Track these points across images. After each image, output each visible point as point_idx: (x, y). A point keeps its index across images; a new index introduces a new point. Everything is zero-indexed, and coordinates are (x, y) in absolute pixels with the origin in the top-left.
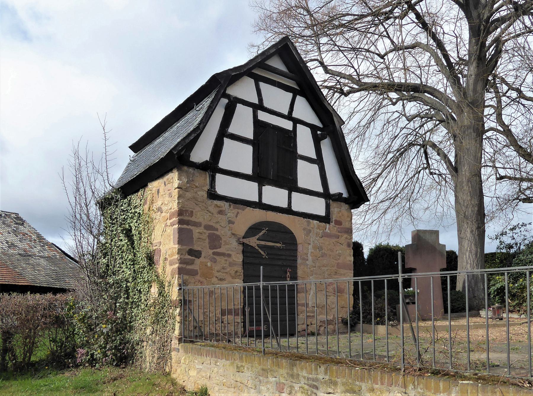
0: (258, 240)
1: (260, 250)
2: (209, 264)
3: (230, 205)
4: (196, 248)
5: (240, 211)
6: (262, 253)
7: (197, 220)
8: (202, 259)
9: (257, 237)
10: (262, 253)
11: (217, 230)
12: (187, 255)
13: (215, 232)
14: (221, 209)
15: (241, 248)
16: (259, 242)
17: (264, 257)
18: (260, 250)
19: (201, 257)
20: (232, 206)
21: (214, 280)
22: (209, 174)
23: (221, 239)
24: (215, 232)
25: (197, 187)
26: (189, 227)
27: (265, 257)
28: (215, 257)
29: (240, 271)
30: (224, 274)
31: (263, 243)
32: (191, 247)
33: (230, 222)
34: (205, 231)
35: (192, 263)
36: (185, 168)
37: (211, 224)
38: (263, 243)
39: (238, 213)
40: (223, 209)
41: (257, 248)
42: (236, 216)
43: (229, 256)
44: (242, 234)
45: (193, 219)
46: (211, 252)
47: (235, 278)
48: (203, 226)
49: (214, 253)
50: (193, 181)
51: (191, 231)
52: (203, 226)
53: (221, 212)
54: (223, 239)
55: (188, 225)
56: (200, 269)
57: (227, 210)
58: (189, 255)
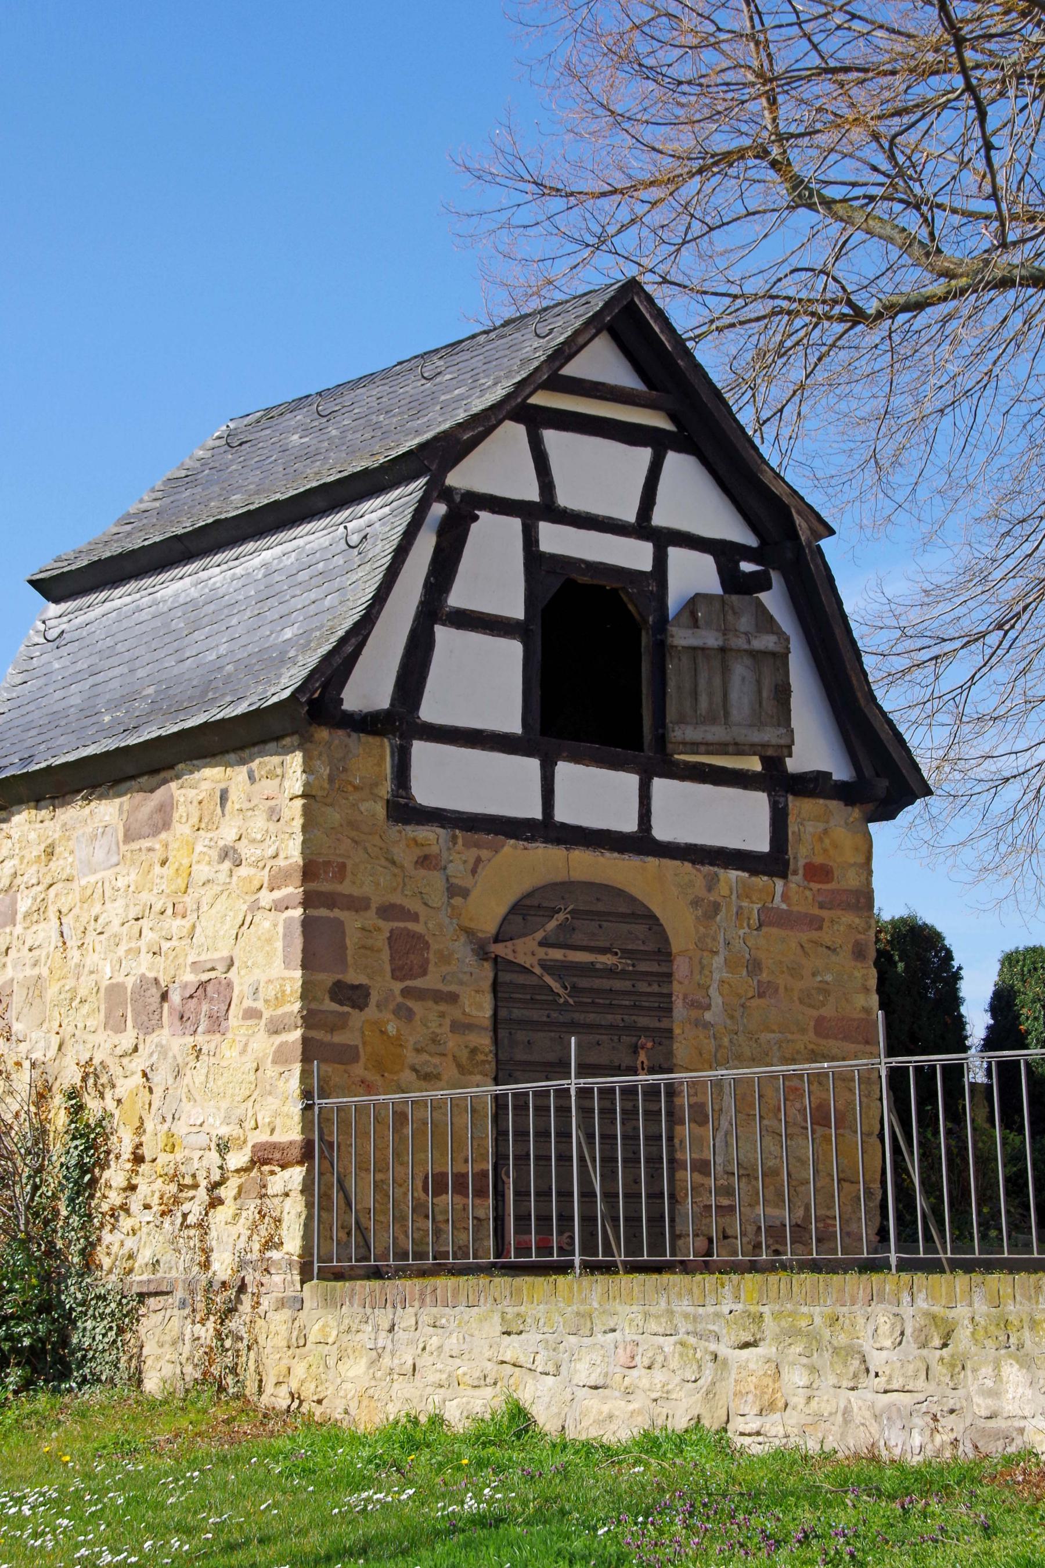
0: (541, 944)
1: (548, 979)
2: (391, 1029)
3: (454, 838)
4: (353, 977)
5: (485, 854)
6: (555, 985)
7: (356, 892)
8: (371, 1012)
9: (539, 935)
10: (555, 985)
11: (415, 917)
12: (327, 1001)
13: (411, 926)
14: (427, 851)
15: (487, 971)
16: (541, 952)
17: (562, 1001)
18: (548, 979)
19: (367, 1005)
20: (460, 841)
21: (408, 1076)
22: (391, 745)
23: (427, 946)
24: (411, 926)
25: (356, 788)
26: (336, 913)
27: (566, 1001)
28: (410, 1003)
29: (487, 1050)
30: (436, 1060)
31: (557, 954)
32: (340, 977)
33: (454, 891)
34: (381, 923)
35: (339, 1024)
36: (323, 734)
37: (397, 899)
38: (557, 954)
39: (478, 860)
40: (434, 849)
41: (538, 970)
42: (474, 872)
43: (453, 998)
44: (489, 926)
45: (346, 888)
46: (398, 986)
47: (471, 1073)
48: (374, 907)
49: (406, 992)
50: (345, 770)
51: (339, 924)
52: (374, 907)
53: (425, 861)
54: (434, 946)
55: (331, 906)
56: (364, 1043)
57: (445, 854)
58: (332, 999)
